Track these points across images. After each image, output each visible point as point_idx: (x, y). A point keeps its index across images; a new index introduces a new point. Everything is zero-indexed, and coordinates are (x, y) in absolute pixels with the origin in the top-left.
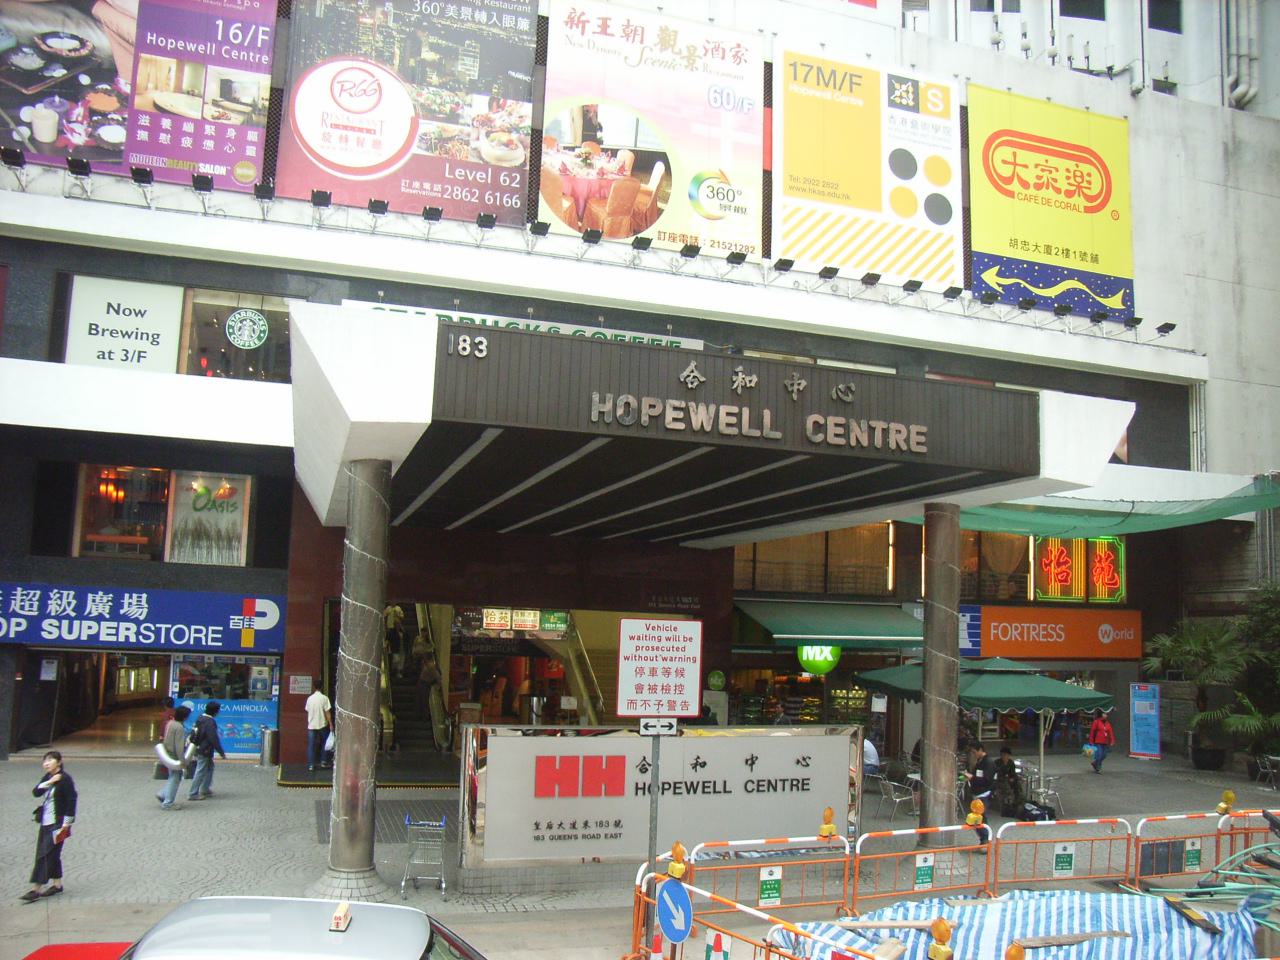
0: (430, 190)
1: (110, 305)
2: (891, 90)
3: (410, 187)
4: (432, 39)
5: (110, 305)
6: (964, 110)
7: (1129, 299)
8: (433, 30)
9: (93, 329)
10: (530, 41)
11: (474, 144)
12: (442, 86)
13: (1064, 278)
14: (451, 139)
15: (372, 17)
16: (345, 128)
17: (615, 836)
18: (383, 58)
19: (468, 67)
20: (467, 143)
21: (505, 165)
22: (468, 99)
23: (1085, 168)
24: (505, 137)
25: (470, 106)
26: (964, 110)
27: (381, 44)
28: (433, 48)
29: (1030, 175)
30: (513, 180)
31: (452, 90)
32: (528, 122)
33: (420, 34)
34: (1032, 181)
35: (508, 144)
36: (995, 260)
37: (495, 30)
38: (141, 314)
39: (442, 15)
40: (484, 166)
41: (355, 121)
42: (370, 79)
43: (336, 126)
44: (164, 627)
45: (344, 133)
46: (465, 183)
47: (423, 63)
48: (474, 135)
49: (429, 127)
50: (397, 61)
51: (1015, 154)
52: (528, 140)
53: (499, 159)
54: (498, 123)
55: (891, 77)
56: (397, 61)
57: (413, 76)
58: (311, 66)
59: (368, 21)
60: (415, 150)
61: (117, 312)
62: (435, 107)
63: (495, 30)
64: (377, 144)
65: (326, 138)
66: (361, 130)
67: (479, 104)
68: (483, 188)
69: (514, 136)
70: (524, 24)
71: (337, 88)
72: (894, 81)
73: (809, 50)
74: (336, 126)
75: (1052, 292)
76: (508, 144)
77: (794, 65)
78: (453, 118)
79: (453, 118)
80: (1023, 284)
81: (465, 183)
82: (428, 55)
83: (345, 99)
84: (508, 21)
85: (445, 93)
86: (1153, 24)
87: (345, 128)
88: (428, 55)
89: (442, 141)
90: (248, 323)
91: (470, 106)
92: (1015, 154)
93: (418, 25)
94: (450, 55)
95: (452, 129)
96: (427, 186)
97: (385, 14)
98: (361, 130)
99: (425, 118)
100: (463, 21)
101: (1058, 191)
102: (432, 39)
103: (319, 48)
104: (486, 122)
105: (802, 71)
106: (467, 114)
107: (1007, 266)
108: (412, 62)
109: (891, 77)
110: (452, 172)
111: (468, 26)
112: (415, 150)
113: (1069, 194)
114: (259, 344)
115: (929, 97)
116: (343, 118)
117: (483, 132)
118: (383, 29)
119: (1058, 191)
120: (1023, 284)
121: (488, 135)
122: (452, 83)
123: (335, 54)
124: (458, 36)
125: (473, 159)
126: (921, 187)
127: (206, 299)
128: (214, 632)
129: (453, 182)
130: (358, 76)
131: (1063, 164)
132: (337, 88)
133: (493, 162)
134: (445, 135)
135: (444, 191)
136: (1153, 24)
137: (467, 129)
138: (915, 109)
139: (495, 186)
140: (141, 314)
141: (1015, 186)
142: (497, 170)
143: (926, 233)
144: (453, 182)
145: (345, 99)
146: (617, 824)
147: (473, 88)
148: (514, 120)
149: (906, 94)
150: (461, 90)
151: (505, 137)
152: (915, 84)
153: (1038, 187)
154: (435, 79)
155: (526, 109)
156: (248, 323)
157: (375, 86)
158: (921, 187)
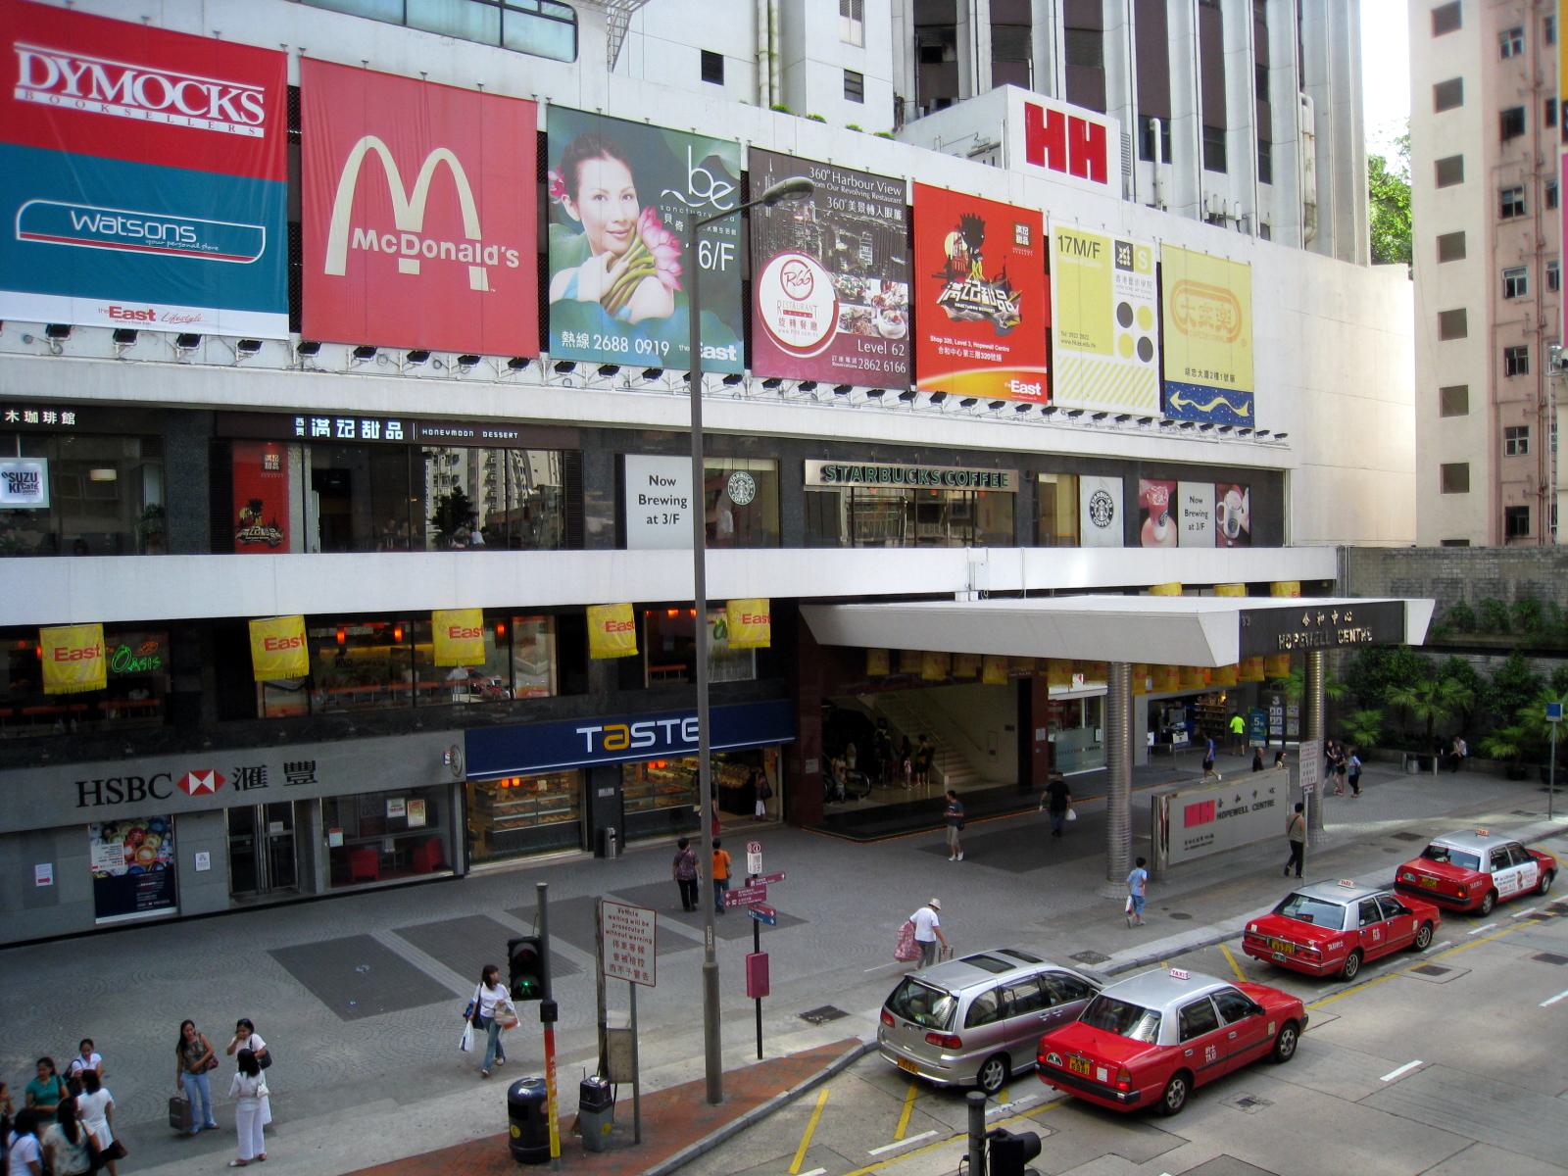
0: (847, 362)
1: (651, 478)
2: (1117, 253)
3: (837, 361)
4: (842, 232)
5: (651, 478)
6: (1159, 265)
7: (1251, 408)
8: (842, 224)
9: (642, 499)
10: (903, 229)
11: (874, 321)
12: (851, 272)
13: (1218, 395)
14: (860, 318)
15: (802, 215)
16: (793, 313)
17: (1210, 843)
18: (811, 251)
19: (866, 255)
20: (870, 321)
21: (895, 337)
22: (868, 282)
23: (1227, 306)
24: (892, 314)
25: (869, 288)
26: (1159, 265)
27: (809, 238)
28: (843, 239)
29: (1195, 315)
30: (900, 349)
31: (858, 276)
32: (906, 300)
33: (833, 227)
34: (1197, 319)
35: (895, 320)
36: (1178, 386)
37: (880, 221)
38: (672, 482)
39: (846, 210)
40: (880, 340)
41: (798, 307)
42: (805, 270)
43: (786, 312)
44: (668, 723)
45: (792, 317)
46: (871, 355)
47: (837, 253)
48: (873, 315)
49: (845, 309)
50: (820, 253)
51: (1187, 299)
52: (906, 315)
53: (891, 333)
54: (887, 302)
55: (1117, 242)
56: (820, 253)
57: (831, 265)
58: (770, 260)
59: (800, 218)
60: (838, 329)
61: (657, 483)
62: (847, 291)
63: (880, 221)
64: (814, 326)
65: (782, 320)
66: (802, 314)
67: (875, 285)
68: (882, 357)
69: (898, 313)
70: (898, 215)
71: (785, 278)
72: (1119, 244)
73: (1072, 228)
74: (786, 312)
75: (1208, 408)
76: (895, 320)
77: (1061, 238)
78: (859, 300)
79: (859, 300)
80: (1194, 403)
81: (871, 355)
82: (840, 246)
83: (790, 288)
84: (888, 212)
85: (853, 279)
86: (1207, 167)
87: (793, 313)
88: (840, 246)
89: (855, 319)
90: (741, 483)
91: (869, 288)
92: (1187, 299)
93: (831, 219)
94: (853, 244)
95: (861, 309)
96: (848, 360)
97: (810, 211)
98: (802, 314)
99: (843, 301)
100: (860, 214)
101: (1212, 326)
102: (842, 232)
103: (770, 244)
104: (880, 301)
105: (1066, 241)
106: (869, 295)
107: (1186, 390)
108: (830, 253)
109: (1117, 242)
110: (862, 347)
111: (864, 218)
112: (838, 329)
113: (1218, 328)
114: (750, 499)
115: (1138, 255)
116: (791, 305)
117: (879, 311)
118: (808, 224)
119: (1212, 326)
120: (1194, 403)
121: (882, 313)
122: (857, 271)
123: (783, 249)
124: (857, 227)
125: (875, 335)
126: (1136, 332)
127: (710, 464)
128: (688, 725)
129: (864, 355)
130: (797, 267)
131: (1215, 304)
132: (785, 278)
133: (886, 336)
134: (856, 315)
135: (858, 362)
136: (1207, 167)
137: (869, 309)
138: (1130, 268)
139: (889, 356)
140: (672, 482)
141: (1189, 326)
142: (890, 342)
143: (1139, 368)
144: (864, 355)
145: (790, 288)
146: (1212, 836)
147: (871, 273)
148: (897, 299)
149: (1125, 255)
150: (861, 275)
151: (892, 314)
152: (1131, 246)
153: (1201, 324)
154: (845, 267)
155: (903, 289)
156: (741, 483)
157: (808, 275)
158: (1136, 332)
